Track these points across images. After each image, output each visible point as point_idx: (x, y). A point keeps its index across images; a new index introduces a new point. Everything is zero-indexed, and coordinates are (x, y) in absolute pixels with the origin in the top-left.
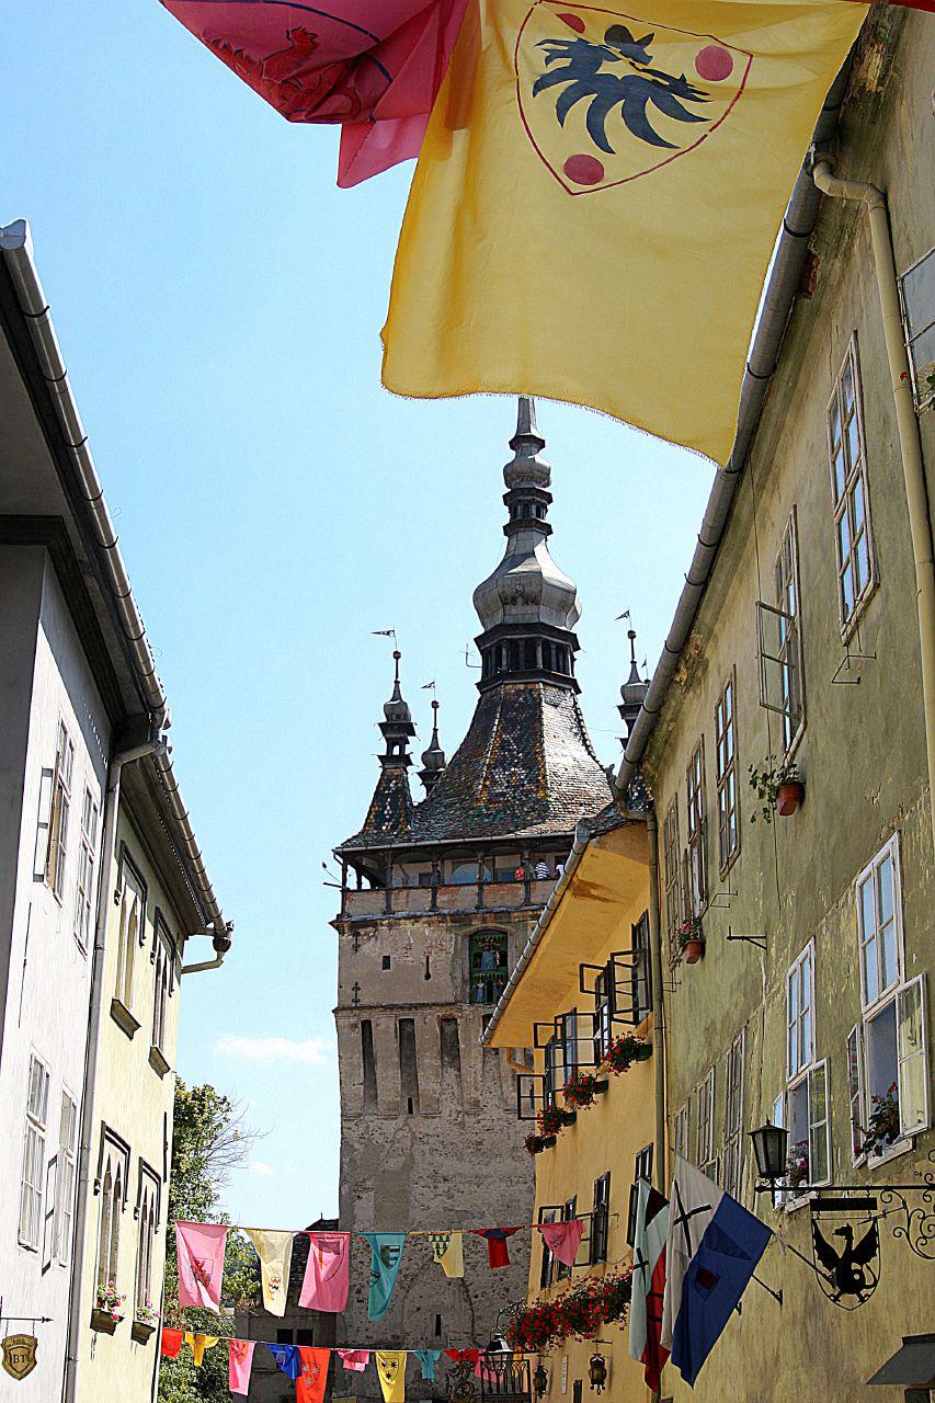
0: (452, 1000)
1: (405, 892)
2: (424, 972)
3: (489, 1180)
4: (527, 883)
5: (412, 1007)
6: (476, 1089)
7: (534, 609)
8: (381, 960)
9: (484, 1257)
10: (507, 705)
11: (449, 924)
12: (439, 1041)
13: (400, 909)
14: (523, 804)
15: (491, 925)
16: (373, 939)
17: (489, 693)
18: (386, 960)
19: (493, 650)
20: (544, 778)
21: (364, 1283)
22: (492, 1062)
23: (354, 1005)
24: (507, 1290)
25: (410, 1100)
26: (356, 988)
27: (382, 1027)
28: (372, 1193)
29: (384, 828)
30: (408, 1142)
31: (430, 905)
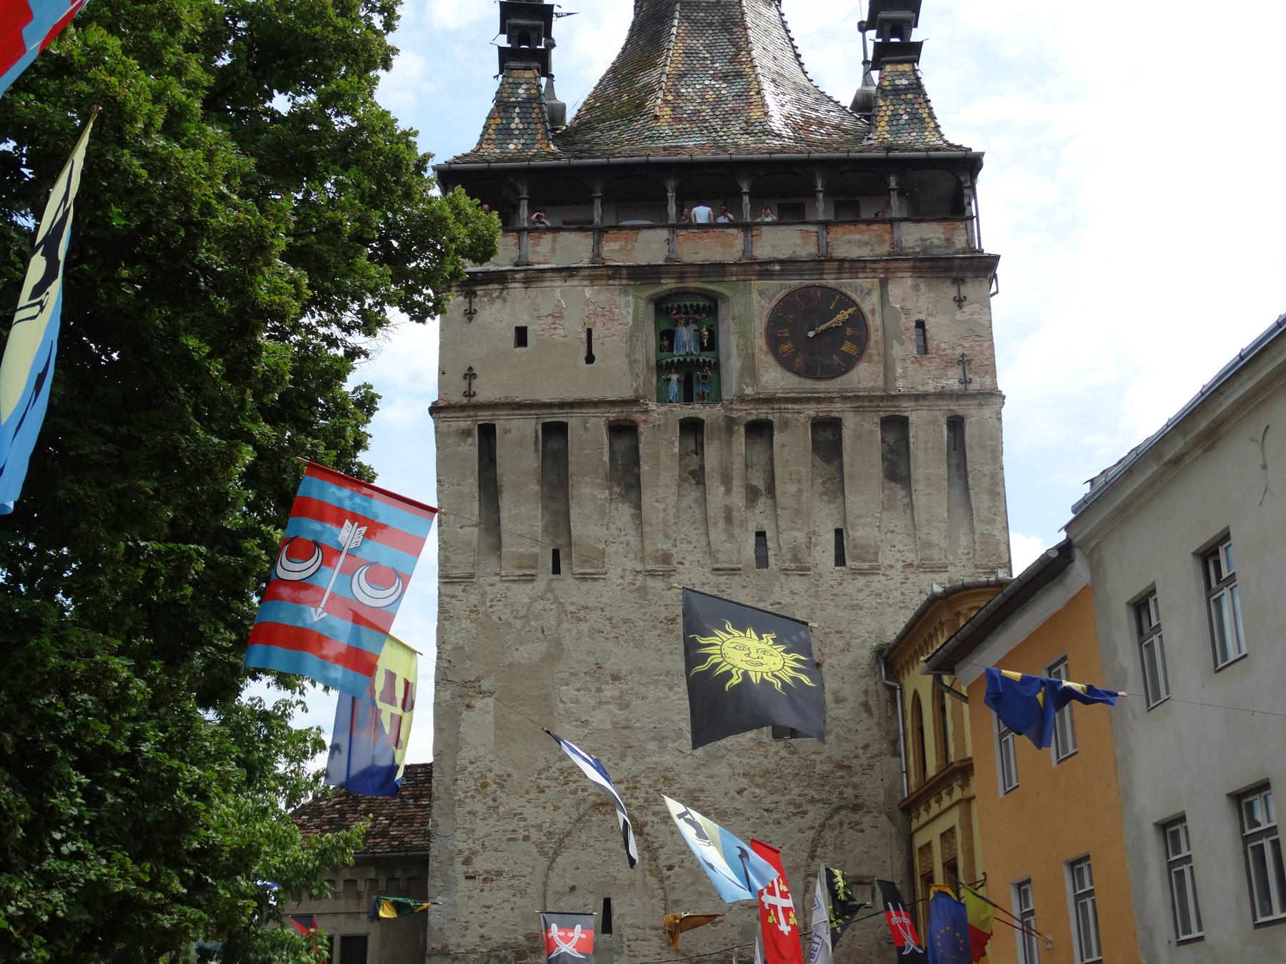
0: (628, 394)
1: (548, 238)
2: (583, 354)
4: (746, 227)
5: (562, 405)
6: (667, 536)
8: (511, 334)
11: (624, 282)
12: (606, 458)
13: (542, 259)
15: (692, 284)
16: (498, 303)
18: (521, 336)
21: (478, 848)
22: (692, 494)
23: (465, 401)
25: (556, 553)
26: (470, 375)
27: (515, 434)
28: (490, 701)
29: (512, 146)
30: (554, 622)
31: (590, 255)
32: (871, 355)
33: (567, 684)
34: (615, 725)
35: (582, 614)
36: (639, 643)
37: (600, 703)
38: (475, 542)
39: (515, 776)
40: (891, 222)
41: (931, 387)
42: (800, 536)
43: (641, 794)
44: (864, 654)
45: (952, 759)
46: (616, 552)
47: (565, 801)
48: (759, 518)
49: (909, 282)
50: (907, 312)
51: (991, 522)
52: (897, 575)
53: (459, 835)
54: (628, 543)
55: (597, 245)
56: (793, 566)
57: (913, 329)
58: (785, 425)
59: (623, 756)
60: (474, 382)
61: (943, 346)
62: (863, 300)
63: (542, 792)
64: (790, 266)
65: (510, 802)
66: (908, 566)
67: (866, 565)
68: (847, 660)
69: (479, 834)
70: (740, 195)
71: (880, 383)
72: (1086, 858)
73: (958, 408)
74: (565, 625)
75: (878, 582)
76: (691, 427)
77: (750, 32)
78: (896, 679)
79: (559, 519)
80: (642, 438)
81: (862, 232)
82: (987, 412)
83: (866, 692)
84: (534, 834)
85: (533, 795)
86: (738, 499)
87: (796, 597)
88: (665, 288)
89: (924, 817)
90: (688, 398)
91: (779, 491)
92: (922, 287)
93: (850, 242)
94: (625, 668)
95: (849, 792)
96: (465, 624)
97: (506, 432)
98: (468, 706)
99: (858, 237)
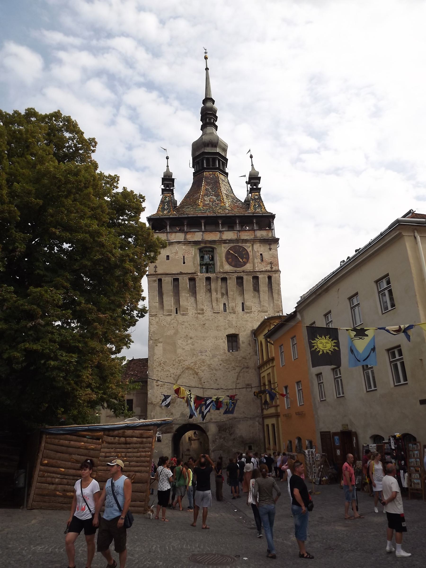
0: (193, 271)
1: (174, 234)
3: (208, 338)
4: (220, 232)
5: (177, 274)
7: (215, 149)
9: (207, 367)
10: (207, 178)
14: (216, 207)
17: (199, 175)
19: (200, 161)
20: (223, 199)
23: (155, 273)
24: (216, 380)
25: (176, 309)
28: (161, 344)
29: (165, 212)
30: (176, 325)
31: (184, 238)
32: (250, 262)
33: (180, 340)
34: (191, 349)
35: (183, 323)
36: (196, 330)
37: (187, 345)
38: (158, 307)
39: (167, 362)
40: (254, 230)
41: (264, 270)
42: (234, 304)
43: (197, 366)
44: (249, 332)
45: (270, 357)
46: (191, 309)
47: (179, 367)
48: (224, 300)
49: (258, 245)
50: (258, 252)
51: (278, 301)
52: (256, 313)
53: (155, 376)
54: (193, 306)
55: (185, 235)
56: (232, 311)
57: (259, 256)
58: (230, 278)
59: (193, 357)
60: (157, 269)
61: (267, 260)
62: (248, 249)
63: (174, 365)
64: (231, 241)
65: (167, 368)
66: (259, 311)
67: (249, 311)
68: (245, 333)
69: (159, 375)
70: (219, 224)
71: (252, 268)
72: (300, 381)
73: (269, 274)
74: (179, 326)
75: (252, 315)
76: (208, 279)
77: (221, 185)
78: (256, 338)
79: (177, 301)
80: (197, 282)
81: (248, 233)
82: (277, 275)
83: (249, 341)
84: (172, 375)
85: (172, 366)
86: (219, 296)
87: (233, 319)
88: (202, 246)
89: (263, 370)
90: (207, 272)
91: (229, 294)
92: (262, 246)
93: (245, 235)
94: (193, 336)
95: (246, 364)
96: (155, 326)
97: (165, 280)
98: (156, 345)
99: (246, 234)
